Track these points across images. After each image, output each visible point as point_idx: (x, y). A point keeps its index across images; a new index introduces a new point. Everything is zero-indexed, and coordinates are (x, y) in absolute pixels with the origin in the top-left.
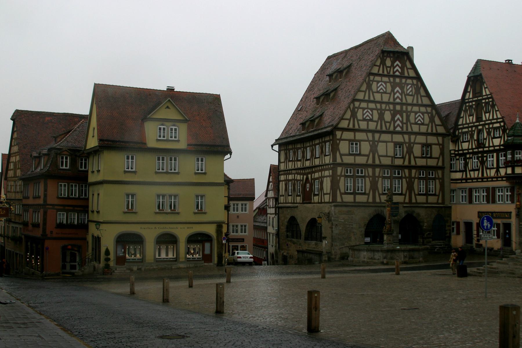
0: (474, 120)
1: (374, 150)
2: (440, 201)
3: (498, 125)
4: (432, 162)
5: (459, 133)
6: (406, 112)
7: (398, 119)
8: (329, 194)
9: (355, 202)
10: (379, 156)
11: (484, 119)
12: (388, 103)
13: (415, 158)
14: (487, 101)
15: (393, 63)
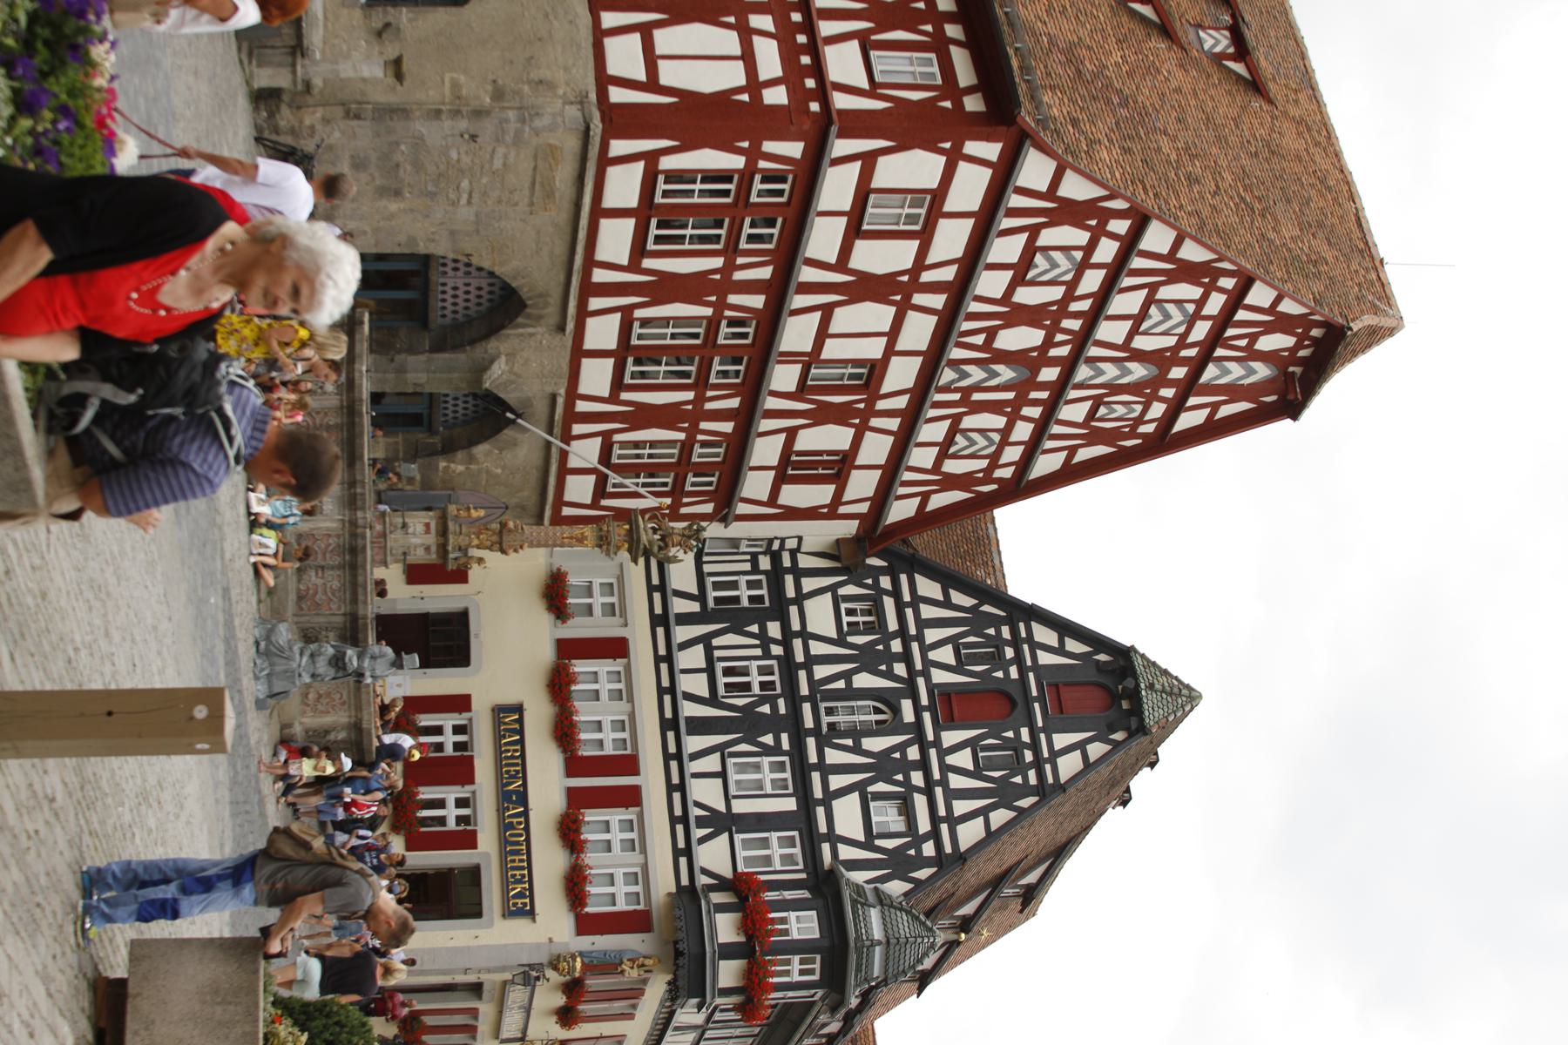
0: (939, 676)
1: (869, 288)
2: (566, 511)
3: (924, 825)
4: (756, 485)
5: (876, 572)
6: (1022, 400)
7: (996, 374)
8: (652, 85)
9: (599, 212)
10: (827, 311)
11: (950, 738)
12: (1083, 338)
13: (792, 433)
14: (1029, 756)
15: (1265, 357)
